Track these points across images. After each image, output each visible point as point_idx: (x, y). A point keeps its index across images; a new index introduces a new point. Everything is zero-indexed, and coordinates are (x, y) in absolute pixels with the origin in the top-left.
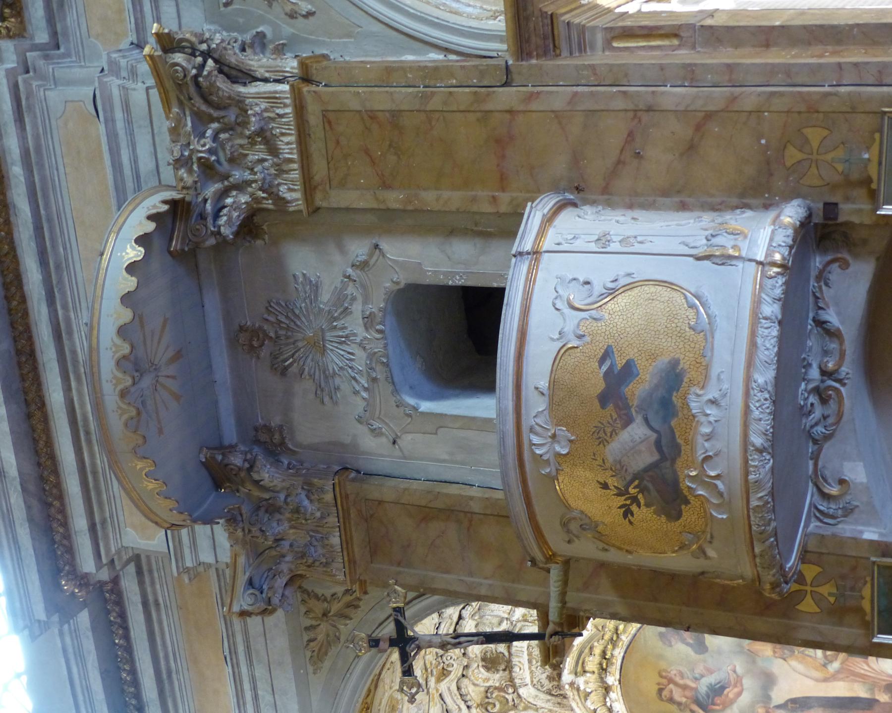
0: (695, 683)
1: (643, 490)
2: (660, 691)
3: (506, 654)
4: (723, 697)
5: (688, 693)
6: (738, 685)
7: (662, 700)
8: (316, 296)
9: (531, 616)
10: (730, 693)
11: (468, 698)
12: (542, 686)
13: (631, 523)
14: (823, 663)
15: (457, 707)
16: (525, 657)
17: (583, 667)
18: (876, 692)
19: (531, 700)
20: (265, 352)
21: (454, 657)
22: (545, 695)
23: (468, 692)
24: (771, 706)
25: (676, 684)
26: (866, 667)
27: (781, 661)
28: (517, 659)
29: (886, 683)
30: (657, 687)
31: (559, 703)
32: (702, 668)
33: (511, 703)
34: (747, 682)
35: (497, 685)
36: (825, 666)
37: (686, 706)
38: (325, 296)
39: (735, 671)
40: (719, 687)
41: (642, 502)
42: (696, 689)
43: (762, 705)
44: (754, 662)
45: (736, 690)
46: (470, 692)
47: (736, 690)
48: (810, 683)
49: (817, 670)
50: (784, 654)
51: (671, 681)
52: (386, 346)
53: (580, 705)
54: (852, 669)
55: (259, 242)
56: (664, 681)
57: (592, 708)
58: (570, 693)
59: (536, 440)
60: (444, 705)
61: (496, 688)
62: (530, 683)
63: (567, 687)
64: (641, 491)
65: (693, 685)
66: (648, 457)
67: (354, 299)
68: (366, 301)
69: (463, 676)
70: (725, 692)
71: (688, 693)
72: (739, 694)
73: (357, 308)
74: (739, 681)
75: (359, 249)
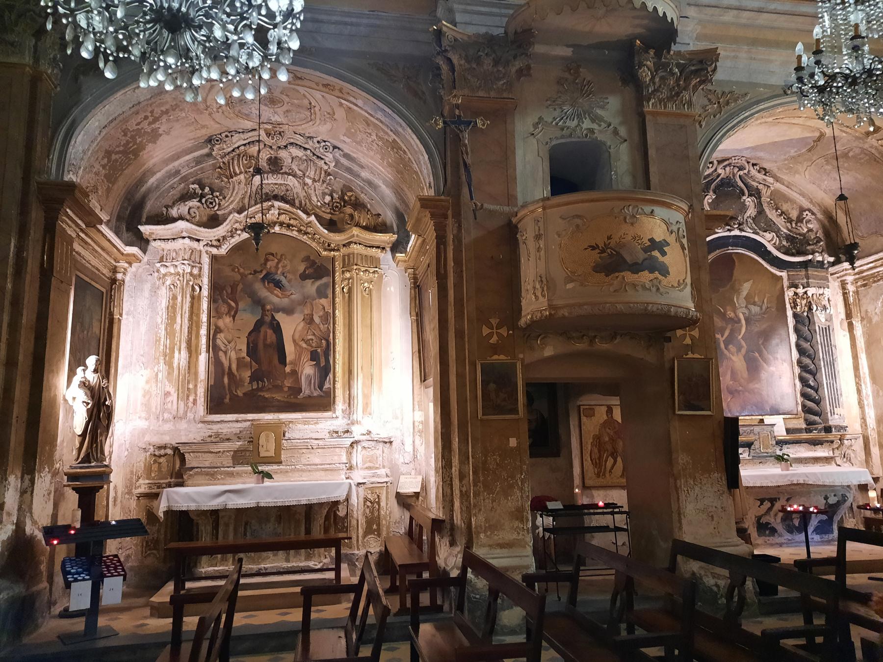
1: (611, 255)
2: (272, 255)
8: (598, 107)
10: (277, 291)
13: (586, 249)
16: (279, 182)
20: (567, 75)
30: (274, 253)
33: (248, 170)
36: (303, 340)
37: (265, 268)
38: (599, 112)
41: (603, 255)
44: (300, 304)
45: (280, 295)
47: (280, 295)
51: (279, 261)
52: (579, 137)
55: (620, 84)
56: (279, 257)
58: (265, 204)
59: (631, 208)
63: (270, 203)
64: (609, 255)
65: (279, 272)
66: (628, 259)
67: (600, 126)
68: (600, 131)
69: (265, 145)
71: (273, 270)
72: (278, 296)
73: (595, 126)
75: (623, 131)
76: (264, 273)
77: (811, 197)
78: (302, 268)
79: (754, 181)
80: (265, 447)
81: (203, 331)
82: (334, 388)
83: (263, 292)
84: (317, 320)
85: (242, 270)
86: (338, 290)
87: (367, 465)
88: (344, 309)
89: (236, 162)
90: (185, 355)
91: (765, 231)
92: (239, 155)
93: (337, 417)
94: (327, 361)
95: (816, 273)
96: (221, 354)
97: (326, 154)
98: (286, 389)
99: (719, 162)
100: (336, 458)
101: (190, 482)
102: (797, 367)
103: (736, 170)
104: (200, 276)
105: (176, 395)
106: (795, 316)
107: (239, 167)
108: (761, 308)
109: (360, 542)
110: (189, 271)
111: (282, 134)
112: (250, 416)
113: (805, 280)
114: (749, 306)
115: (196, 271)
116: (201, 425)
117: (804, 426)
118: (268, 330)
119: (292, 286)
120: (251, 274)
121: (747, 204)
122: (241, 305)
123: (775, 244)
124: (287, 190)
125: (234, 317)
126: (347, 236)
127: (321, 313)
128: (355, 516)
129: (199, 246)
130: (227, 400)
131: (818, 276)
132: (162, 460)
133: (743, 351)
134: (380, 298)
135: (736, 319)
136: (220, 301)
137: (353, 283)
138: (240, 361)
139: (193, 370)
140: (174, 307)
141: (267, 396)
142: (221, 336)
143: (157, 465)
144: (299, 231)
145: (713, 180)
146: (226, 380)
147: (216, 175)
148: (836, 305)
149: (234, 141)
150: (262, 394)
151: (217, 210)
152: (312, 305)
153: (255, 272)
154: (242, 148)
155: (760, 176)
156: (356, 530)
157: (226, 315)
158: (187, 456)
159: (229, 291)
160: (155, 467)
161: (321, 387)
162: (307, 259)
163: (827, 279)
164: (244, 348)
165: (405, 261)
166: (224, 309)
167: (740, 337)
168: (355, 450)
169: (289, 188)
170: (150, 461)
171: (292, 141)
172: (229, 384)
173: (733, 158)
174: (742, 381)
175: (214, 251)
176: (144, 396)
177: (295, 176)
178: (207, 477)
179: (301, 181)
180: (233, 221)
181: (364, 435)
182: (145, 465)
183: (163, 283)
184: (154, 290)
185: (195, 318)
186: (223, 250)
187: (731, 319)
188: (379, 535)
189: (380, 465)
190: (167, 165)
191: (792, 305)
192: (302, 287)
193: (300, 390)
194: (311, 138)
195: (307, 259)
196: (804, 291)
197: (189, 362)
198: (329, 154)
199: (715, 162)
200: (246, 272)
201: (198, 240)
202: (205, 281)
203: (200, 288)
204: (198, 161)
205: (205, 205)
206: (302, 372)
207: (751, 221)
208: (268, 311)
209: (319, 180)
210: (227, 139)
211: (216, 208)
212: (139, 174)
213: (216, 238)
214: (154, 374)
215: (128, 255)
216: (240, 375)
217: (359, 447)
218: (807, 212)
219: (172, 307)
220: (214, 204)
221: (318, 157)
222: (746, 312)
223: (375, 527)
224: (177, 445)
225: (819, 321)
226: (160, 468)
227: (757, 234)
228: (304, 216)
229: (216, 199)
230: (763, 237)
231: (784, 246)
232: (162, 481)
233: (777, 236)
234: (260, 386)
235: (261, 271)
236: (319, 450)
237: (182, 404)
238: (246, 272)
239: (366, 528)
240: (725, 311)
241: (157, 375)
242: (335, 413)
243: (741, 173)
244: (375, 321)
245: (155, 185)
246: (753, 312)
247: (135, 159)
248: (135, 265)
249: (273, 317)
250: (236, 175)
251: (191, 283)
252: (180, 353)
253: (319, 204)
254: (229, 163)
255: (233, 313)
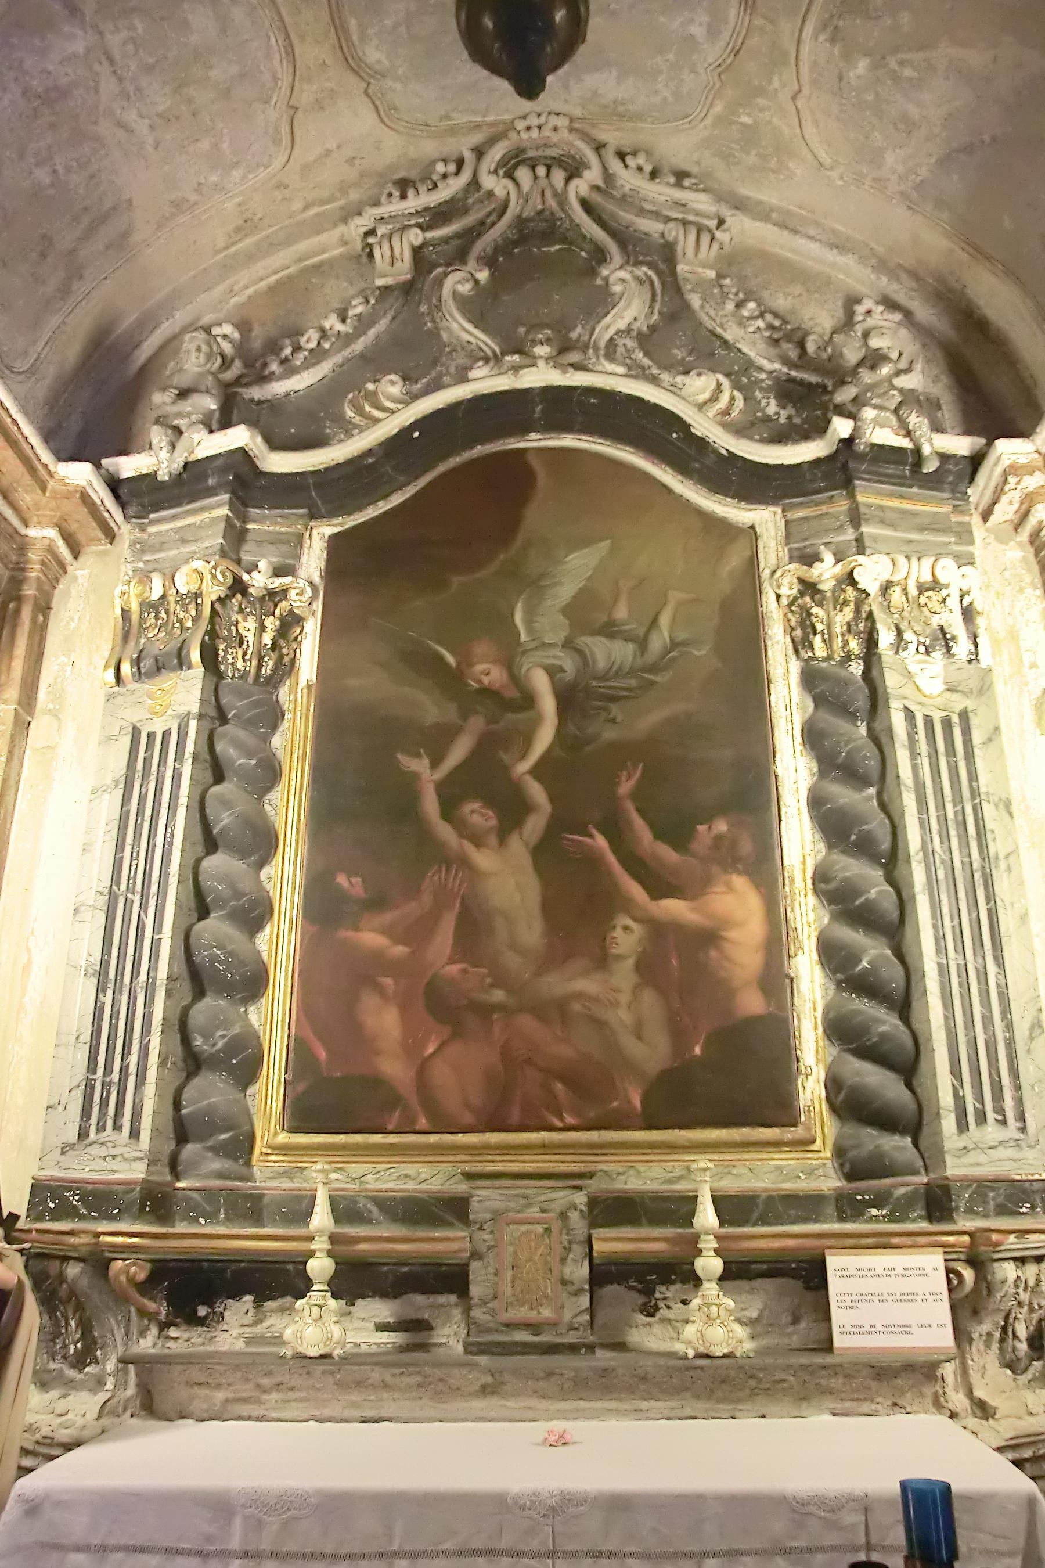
77: (880, 250)
79: (642, 212)
91: (687, 373)
95: (896, 503)
99: (479, 152)
102: (812, 899)
103: (558, 176)
106: (811, 679)
108: (643, 644)
113: (850, 534)
114: (587, 641)
117: (830, 1182)
121: (617, 289)
123: (726, 412)
131: (915, 514)
133: (535, 825)
135: (512, 693)
145: (481, 228)
148: (1013, 635)
155: (660, 192)
163: (965, 534)
167: (523, 767)
173: (520, 125)
174: (512, 961)
187: (487, 693)
191: (798, 633)
196: (839, 569)
199: (468, 156)
207: (630, 343)
218: (868, 304)
222: (569, 664)
225: (908, 691)
227: (654, 380)
230: (674, 390)
231: (767, 419)
233: (737, 386)
240: (466, 660)
243: (580, 187)
246: (601, 664)
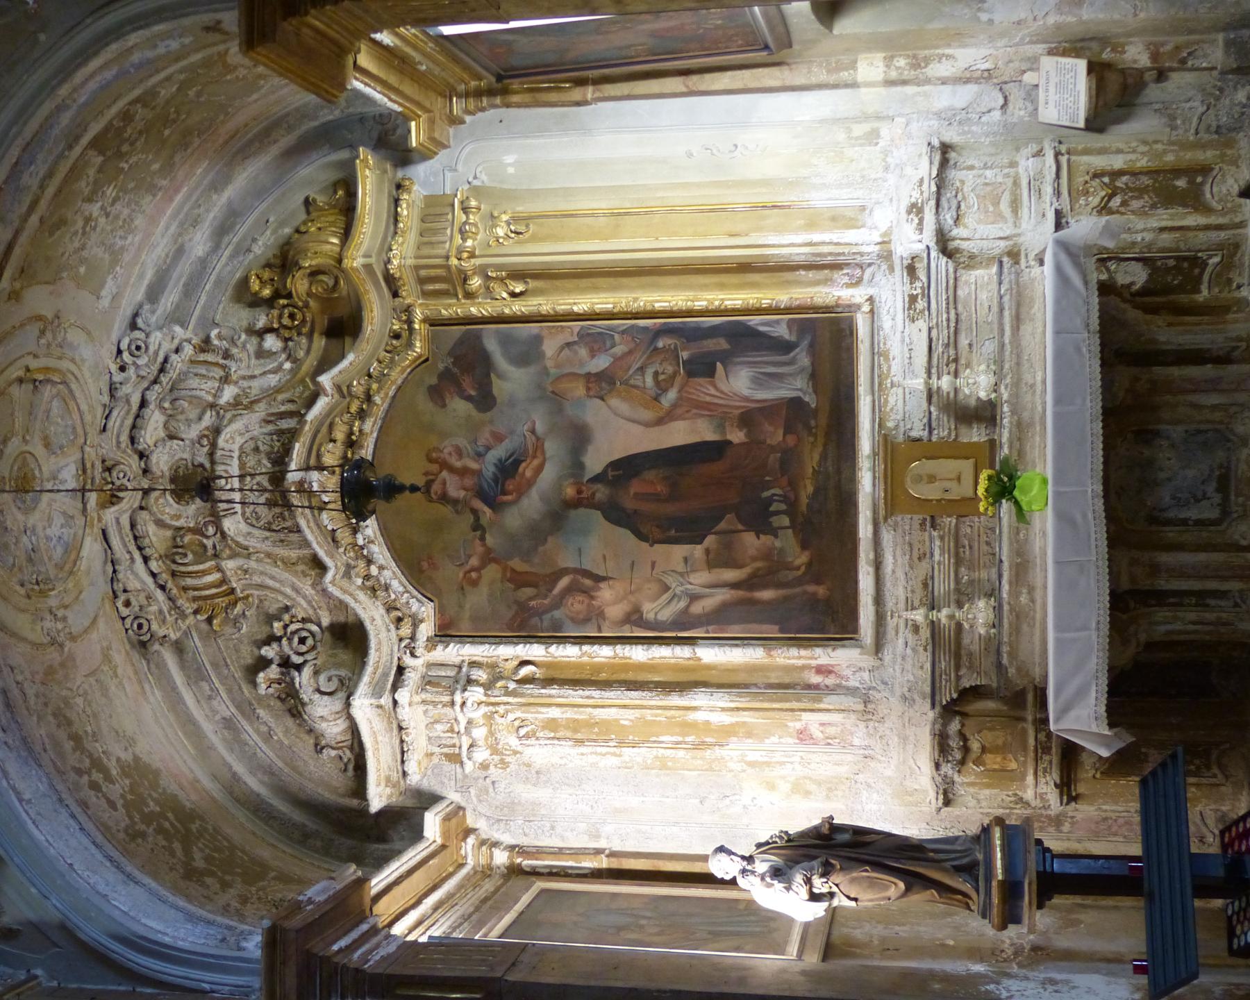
0: (476, 461)
3: (208, 465)
4: (517, 478)
5: (469, 482)
6: (539, 454)
7: (430, 501)
9: (247, 397)
10: (527, 470)
11: (147, 541)
12: (257, 519)
14: (654, 395)
15: (128, 556)
17: (319, 456)
18: (728, 429)
19: (240, 539)
21: (129, 473)
22: (261, 532)
23: (147, 532)
24: (585, 480)
25: (452, 470)
26: (713, 391)
27: (598, 401)
28: (223, 467)
29: (740, 411)
31: (282, 541)
32: (487, 435)
33: (210, 552)
34: (551, 447)
35: (191, 525)
37: (466, 502)
39: (533, 431)
40: (511, 463)
42: (478, 473)
43: (571, 480)
44: (560, 410)
45: (536, 462)
46: (150, 533)
47: (536, 462)
48: (637, 429)
49: (645, 408)
50: (602, 389)
51: (444, 465)
53: (312, 524)
54: (694, 397)
57: (330, 528)
58: (295, 499)
60: (109, 551)
61: (190, 530)
62: (240, 512)
65: (474, 465)
69: (142, 508)
70: (521, 469)
71: (469, 482)
74: (539, 442)
76: (478, 504)
78: (460, 407)
80: (947, 485)
81: (638, 654)
82: (788, 310)
83: (531, 505)
84: (601, 363)
85: (474, 562)
86: (518, 307)
87: (1005, 207)
88: (569, 291)
89: (189, 582)
90: (701, 696)
92: (174, 574)
93: (871, 300)
94: (714, 331)
96: (697, 608)
97: (152, 349)
98: (791, 440)
100: (983, 296)
101: (1037, 672)
104: (493, 666)
105: (806, 716)
107: (204, 573)
109: (1221, 221)
110: (481, 690)
111: (108, 464)
112: (865, 530)
115: (481, 675)
116: (887, 656)
118: (632, 492)
119: (512, 432)
120: (482, 539)
122: (567, 560)
124: (256, 449)
125: (599, 579)
126: (370, 286)
127: (583, 352)
128: (1149, 237)
129: (416, 666)
130: (821, 591)
132: (975, 746)
134: (535, 194)
136: (557, 614)
137: (499, 268)
138: (714, 561)
139: (741, 678)
140: (575, 725)
141: (810, 489)
142: (650, 610)
143: (988, 758)
144: (362, 415)
146: (767, 594)
147: (228, 630)
149: (138, 586)
150: (804, 500)
151: (319, 625)
152: (559, 378)
153: (477, 526)
154: (154, 565)
156: (1191, 234)
157: (592, 598)
158: (966, 683)
159: (529, 591)
160: (993, 761)
161: (785, 347)
162: (437, 394)
164: (680, 551)
165: (432, 122)
166: (576, 604)
168: (964, 245)
169: (251, 444)
170: (977, 774)
171: (124, 438)
172: (779, 585)
175: (426, 630)
176: (808, 793)
177: (217, 431)
178: (1025, 628)
179: (228, 415)
180: (345, 583)
181: (921, 221)
182: (988, 786)
183: (515, 753)
184: (537, 775)
185: (603, 676)
186: (427, 611)
188: (1205, 170)
189: (1007, 176)
190: (211, 747)
192: (512, 403)
193: (795, 404)
194: (112, 389)
195: (437, 394)
197: (720, 686)
198: (151, 340)
200: (480, 549)
201: (401, 670)
202: (508, 653)
203: (524, 663)
204: (196, 674)
205: (308, 657)
206: (746, 399)
208: (579, 492)
209: (224, 367)
210: (134, 602)
211: (314, 628)
212: (241, 815)
213: (392, 627)
214: (750, 770)
215: (446, 834)
216: (754, 559)
217: (955, 232)
219: (575, 731)
220: (304, 634)
221: (162, 370)
223: (1181, 183)
224: (938, 709)
226: (996, 750)
228: (321, 404)
229: (293, 627)
232: (1031, 741)
234: (783, 507)
235: (475, 512)
236: (964, 342)
237: (829, 702)
238: (480, 549)
239: (1185, 205)
241: (752, 764)
242: (859, 307)
244: (601, 204)
245: (266, 779)
247: (202, 819)
248: (470, 821)
249: (596, 479)
250: (224, 581)
251: (512, 686)
252: (695, 709)
253: (287, 366)
254: (195, 599)
255: (588, 582)
